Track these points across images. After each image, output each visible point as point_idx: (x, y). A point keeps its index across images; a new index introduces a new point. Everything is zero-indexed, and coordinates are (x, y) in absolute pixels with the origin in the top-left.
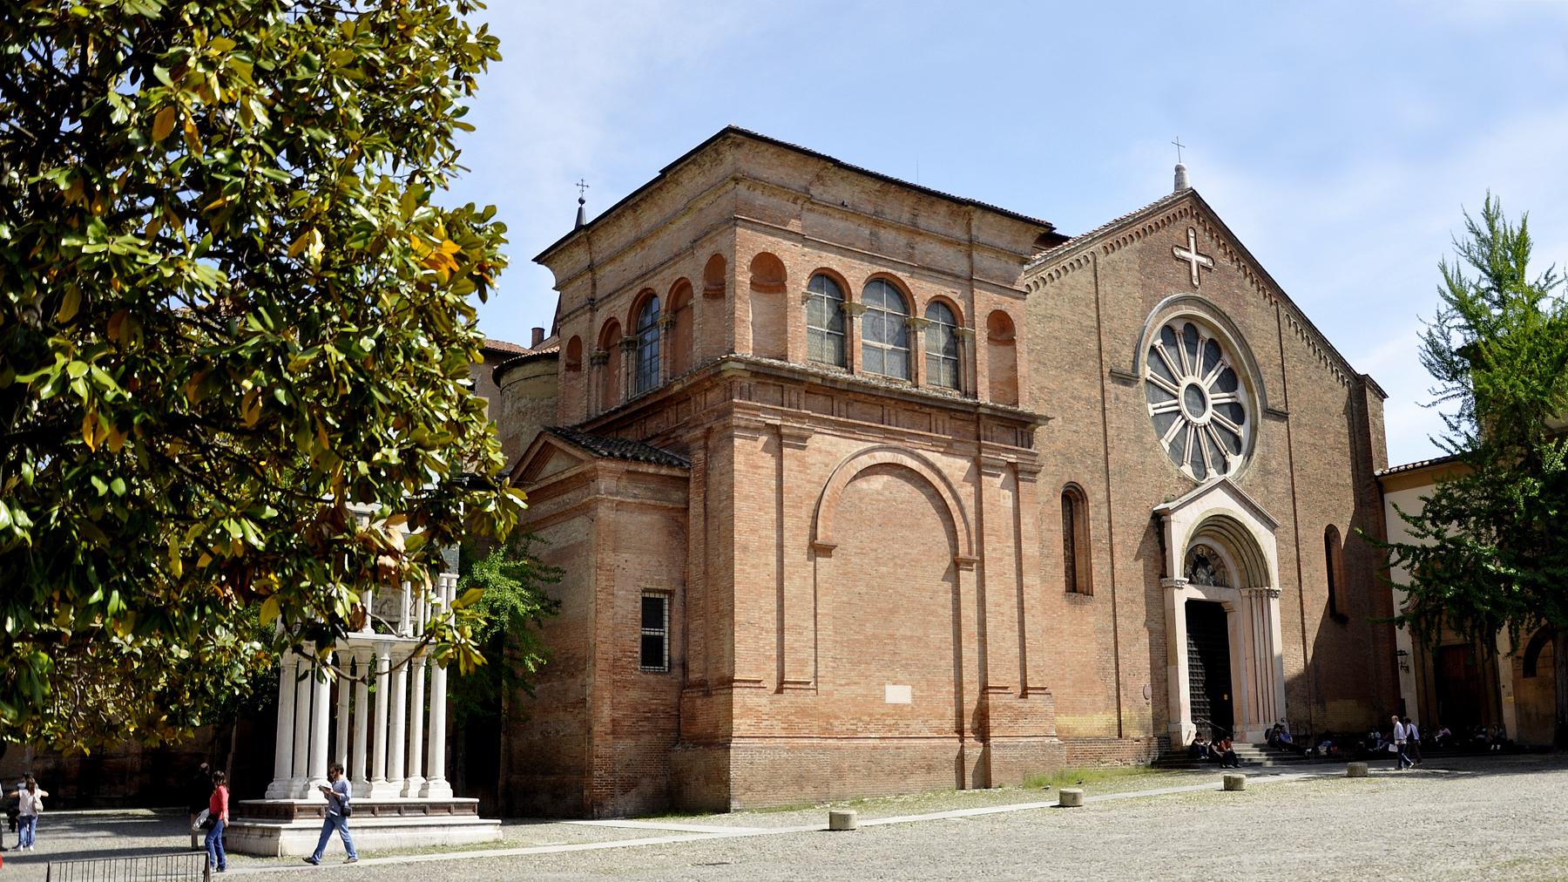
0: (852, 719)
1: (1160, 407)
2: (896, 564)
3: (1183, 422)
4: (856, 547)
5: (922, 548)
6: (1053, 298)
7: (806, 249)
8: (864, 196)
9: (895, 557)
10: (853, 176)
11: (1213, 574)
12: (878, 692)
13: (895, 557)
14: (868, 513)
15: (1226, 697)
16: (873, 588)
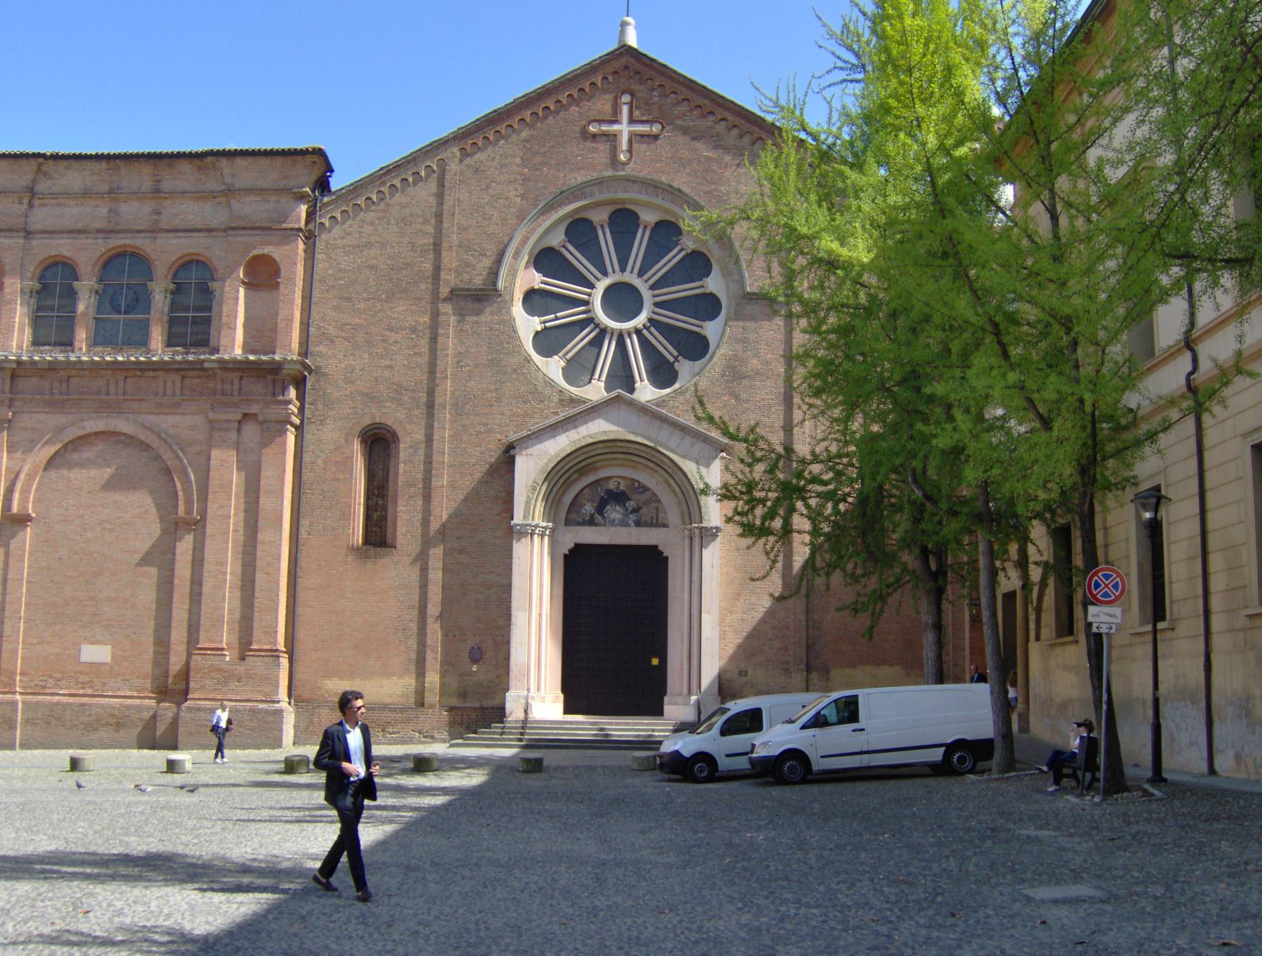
0: (42, 676)
1: (557, 318)
2: (104, 529)
3: (598, 330)
4: (60, 515)
5: (137, 511)
6: (372, 224)
7: (35, 242)
8: (96, 178)
9: (105, 522)
10: (74, 164)
11: (635, 511)
12: (73, 651)
13: (105, 522)
14: (77, 482)
15: (655, 662)
16: (76, 553)
